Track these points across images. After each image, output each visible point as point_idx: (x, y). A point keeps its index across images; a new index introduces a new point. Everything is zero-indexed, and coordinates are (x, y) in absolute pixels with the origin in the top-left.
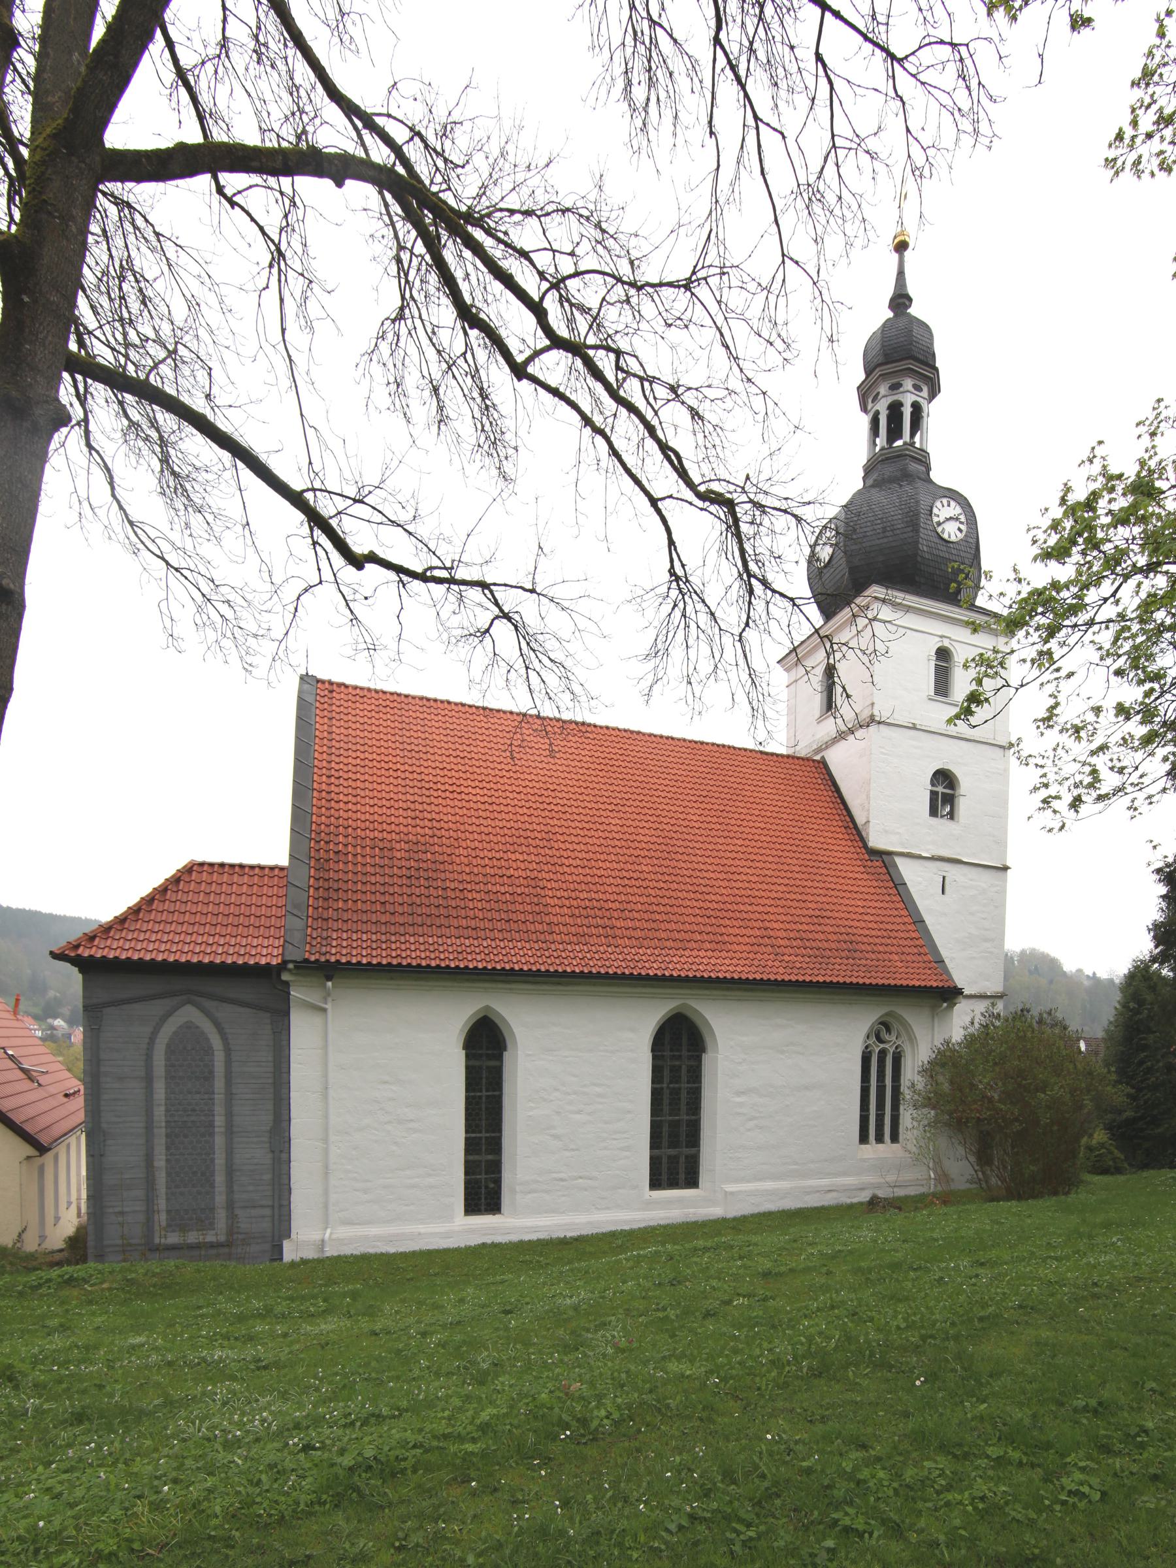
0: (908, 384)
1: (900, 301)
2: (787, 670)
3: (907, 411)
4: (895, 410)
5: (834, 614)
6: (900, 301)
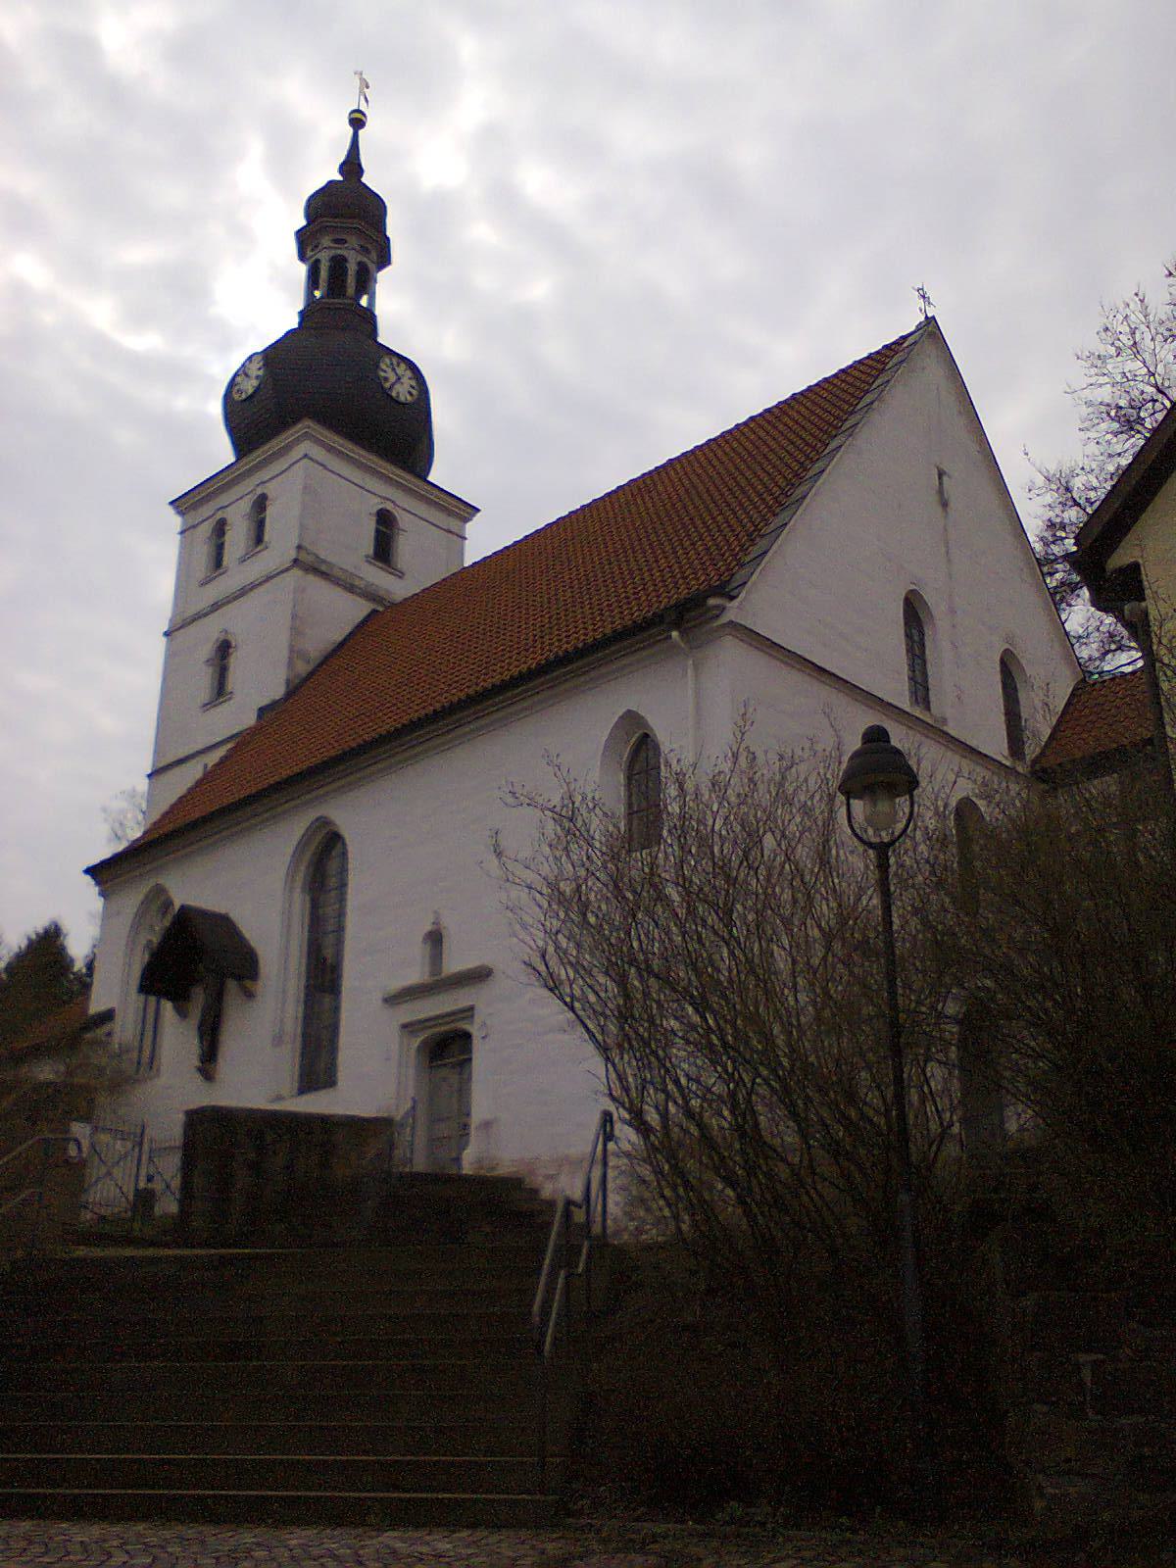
0: (353, 241)
1: (352, 165)
2: (181, 513)
3: (352, 268)
4: (338, 265)
5: (250, 451)
6: (352, 165)
